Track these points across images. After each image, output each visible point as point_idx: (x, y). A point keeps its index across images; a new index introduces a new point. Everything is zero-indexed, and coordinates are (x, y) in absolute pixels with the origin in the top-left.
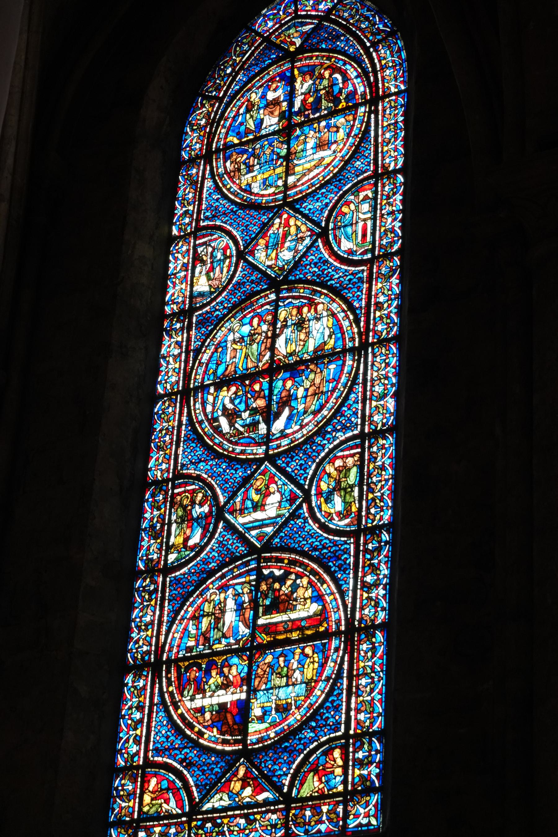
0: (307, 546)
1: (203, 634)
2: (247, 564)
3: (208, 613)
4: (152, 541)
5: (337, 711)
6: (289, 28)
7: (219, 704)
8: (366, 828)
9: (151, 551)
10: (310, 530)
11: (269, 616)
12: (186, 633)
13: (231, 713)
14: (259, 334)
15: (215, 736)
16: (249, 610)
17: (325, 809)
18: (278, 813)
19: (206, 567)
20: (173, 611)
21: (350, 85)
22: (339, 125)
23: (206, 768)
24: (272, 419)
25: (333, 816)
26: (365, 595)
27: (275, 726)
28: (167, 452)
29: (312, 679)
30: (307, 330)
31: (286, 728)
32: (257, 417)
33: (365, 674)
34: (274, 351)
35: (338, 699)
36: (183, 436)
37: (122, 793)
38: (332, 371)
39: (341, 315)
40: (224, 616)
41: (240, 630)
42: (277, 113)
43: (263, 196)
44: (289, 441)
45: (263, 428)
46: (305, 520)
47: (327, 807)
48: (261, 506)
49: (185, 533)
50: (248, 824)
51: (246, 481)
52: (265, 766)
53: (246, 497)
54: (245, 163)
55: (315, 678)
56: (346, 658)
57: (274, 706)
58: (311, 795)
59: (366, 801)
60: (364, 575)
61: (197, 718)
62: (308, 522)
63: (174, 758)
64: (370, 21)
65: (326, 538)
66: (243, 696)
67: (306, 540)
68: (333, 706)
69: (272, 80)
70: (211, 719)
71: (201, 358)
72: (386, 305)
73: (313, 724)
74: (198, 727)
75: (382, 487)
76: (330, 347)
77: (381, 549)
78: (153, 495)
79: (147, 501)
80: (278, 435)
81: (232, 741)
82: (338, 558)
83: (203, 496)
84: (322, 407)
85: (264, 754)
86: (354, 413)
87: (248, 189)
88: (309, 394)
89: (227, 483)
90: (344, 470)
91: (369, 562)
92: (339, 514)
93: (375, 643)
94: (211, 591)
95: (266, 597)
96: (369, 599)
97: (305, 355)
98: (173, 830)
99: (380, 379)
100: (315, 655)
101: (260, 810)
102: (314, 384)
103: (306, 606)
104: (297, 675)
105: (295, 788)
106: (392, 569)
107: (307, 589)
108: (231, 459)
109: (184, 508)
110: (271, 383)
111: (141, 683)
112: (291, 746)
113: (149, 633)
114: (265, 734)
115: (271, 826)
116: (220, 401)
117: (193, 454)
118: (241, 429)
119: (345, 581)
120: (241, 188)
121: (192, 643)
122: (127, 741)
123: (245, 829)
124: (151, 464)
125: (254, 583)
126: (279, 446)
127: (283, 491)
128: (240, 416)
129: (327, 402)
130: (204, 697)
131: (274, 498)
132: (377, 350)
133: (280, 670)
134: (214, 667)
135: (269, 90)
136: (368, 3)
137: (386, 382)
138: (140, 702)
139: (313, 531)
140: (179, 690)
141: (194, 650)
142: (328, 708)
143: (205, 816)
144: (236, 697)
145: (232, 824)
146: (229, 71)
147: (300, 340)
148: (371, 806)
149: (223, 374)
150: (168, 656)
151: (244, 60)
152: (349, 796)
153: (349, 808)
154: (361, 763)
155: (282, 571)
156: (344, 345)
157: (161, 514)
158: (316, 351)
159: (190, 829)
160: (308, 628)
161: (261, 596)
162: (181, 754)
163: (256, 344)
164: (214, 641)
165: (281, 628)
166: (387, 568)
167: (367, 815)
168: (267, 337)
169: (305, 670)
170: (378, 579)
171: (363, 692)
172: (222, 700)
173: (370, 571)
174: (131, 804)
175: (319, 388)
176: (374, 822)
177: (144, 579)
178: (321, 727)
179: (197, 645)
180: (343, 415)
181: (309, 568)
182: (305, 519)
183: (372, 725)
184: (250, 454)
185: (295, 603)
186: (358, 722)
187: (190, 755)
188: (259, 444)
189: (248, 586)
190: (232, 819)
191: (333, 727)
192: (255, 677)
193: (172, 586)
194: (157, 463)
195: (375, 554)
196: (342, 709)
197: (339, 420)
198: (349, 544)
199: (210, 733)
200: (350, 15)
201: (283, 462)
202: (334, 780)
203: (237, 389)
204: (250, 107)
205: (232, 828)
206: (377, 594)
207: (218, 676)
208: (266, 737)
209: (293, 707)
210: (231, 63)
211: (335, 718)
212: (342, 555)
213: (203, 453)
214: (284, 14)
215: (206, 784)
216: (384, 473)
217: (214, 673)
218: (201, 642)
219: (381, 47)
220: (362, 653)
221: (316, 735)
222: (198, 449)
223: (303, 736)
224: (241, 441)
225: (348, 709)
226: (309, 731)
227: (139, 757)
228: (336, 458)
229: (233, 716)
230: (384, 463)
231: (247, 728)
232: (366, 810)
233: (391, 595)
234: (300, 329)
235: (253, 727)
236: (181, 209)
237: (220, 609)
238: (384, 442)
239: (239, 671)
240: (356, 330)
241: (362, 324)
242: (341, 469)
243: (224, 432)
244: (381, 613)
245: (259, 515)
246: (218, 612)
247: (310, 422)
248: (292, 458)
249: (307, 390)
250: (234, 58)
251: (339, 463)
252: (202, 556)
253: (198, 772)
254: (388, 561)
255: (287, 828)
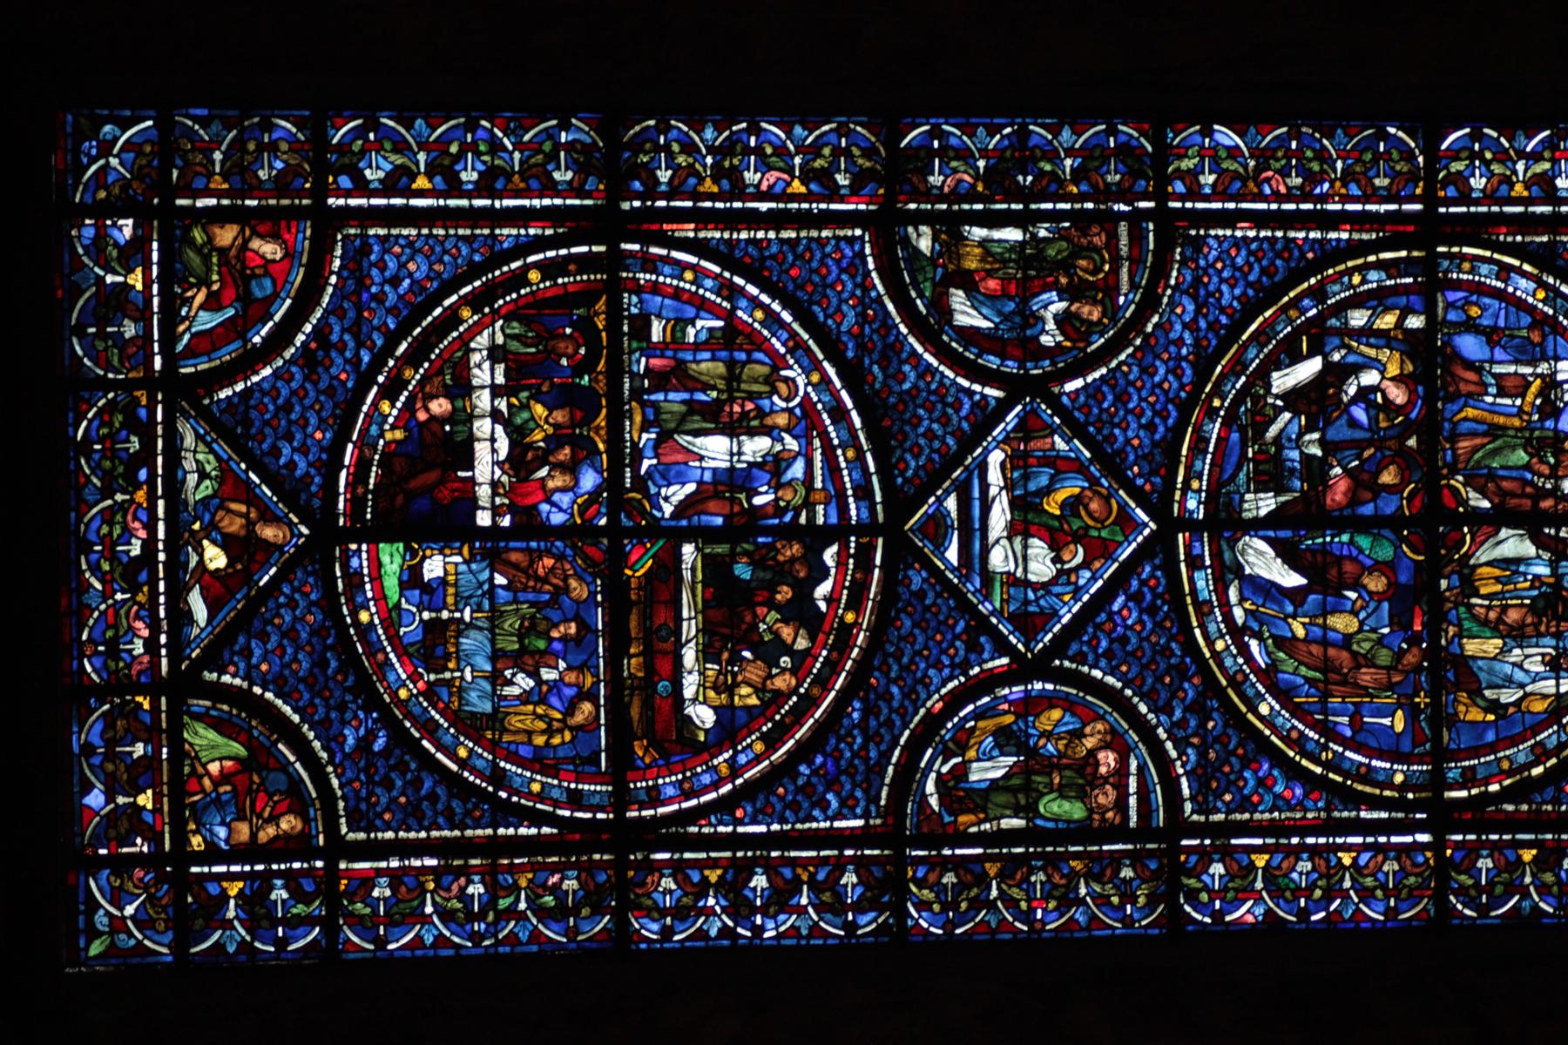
0: (883, 681)
1: (680, 368)
2: (863, 492)
3: (739, 379)
4: (981, 164)
5: (406, 816)
7: (471, 439)
8: (81, 924)
9: (954, 164)
10: (927, 686)
11: (700, 576)
12: (690, 312)
13: (442, 482)
14: (1554, 468)
15: (381, 435)
16: (726, 511)
17: (145, 800)
18: (146, 659)
19: (875, 356)
20: (763, 259)
23: (293, 416)
24: (1282, 534)
25: (124, 826)
26: (713, 875)
27: (391, 624)
28: (1251, 184)
29: (504, 730)
30: (1529, 630)
31: (380, 657)
32: (1297, 484)
33: (494, 890)
34: (1489, 525)
35: (436, 813)
36: (1292, 234)
37: (252, 146)
38: (1387, 721)
39: (1548, 736)
40: (721, 432)
41: (673, 489)
44: (1203, 595)
45: (1265, 504)
46: (959, 665)
47: (150, 806)
48: (1026, 522)
49: (989, 274)
50: (125, 566)
51: (1111, 462)
52: (281, 606)
53: (1061, 466)
55: (506, 738)
56: (546, 830)
57: (445, 615)
58: (187, 755)
59: (153, 921)
60: (771, 868)
61: (441, 372)
62: (951, 678)
63: (334, 310)
65: (895, 742)
66: (484, 519)
67: (899, 677)
68: (421, 800)
70: (432, 418)
71: (1524, 274)
72: (1549, 878)
73: (379, 744)
74: (414, 377)
75: (1012, 904)
76: (1462, 708)
77: (836, 914)
78: (1126, 151)
79: (1112, 131)
80: (1227, 556)
81: (360, 490)
82: (832, 784)
83: (1090, 323)
84: (1284, 695)
85: (313, 597)
86: (1248, 798)
88: (1332, 652)
89: (1117, 398)
90: (1082, 778)
91: (805, 877)
92: (961, 772)
93: (577, 915)
94: (801, 381)
95: (756, 563)
96: (703, 888)
97: (1452, 630)
98: (130, 330)
99: (1329, 877)
100: (568, 736)
101: (162, 599)
102: (1359, 667)
103: (711, 694)
104: (524, 682)
105: (208, 703)
106: (776, 951)
107: (759, 690)
108: (1185, 409)
109: (1066, 265)
110: (1394, 523)
111: (562, 176)
112: (327, 678)
113: (709, 186)
114: (370, 595)
115: (116, 638)
116: (1372, 352)
117: (1225, 274)
118: (1272, 431)
119: (762, 811)
121: (657, 331)
122: (401, 147)
123: (113, 557)
124: (1226, 136)
125: (803, 520)
126: (1195, 563)
127: (1057, 589)
128: (1310, 428)
129: (1297, 711)
130: (496, 391)
131: (1041, 567)
132: (1421, 859)
133: (542, 626)
134: (579, 415)
137: (1318, 893)
138: (508, 175)
139: (923, 696)
140: (527, 306)
141: (635, 345)
142: (417, 783)
143: (160, 430)
144: (484, 492)
145: (129, 518)
147: (1505, 609)
148: (140, 937)
149: (1458, 357)
150: (631, 253)
152: (172, 866)
153: (138, 873)
154: (255, 903)
155: (823, 606)
156: (1458, 755)
157: (1061, 183)
158: (1463, 663)
159: (128, 386)
160: (648, 704)
161: (759, 546)
162: (343, 331)
163: (1526, 458)
164: (654, 404)
165: (662, 616)
166: (779, 936)
167: (117, 925)
168: (1542, 493)
169: (531, 707)
170: (755, 910)
171: (449, 890)
172: (482, 450)
173: (780, 883)
174: (218, 183)
175: (1344, 683)
176: (96, 948)
177: (869, 152)
178: (366, 770)
179: (650, 350)
180: (1246, 763)
181: (816, 691)
182: (965, 666)
183: (357, 922)
184: (1188, 468)
185: (725, 655)
186: (368, 881)
187: (339, 361)
188: (1210, 502)
189: (798, 501)
190: (143, 516)
191: (363, 806)
192: (529, 550)
193: (837, 248)
194: (1223, 154)
195: (826, 897)
196: (408, 830)
197: (1233, 753)
198: (866, 815)
199: (391, 420)
201: (1143, 583)
202: (218, 819)
203: (1400, 409)
205: (119, 517)
206: (709, 912)
207: (551, 431)
208: (359, 599)
209: (432, 677)
211: (387, 809)
212: (838, 795)
213: (1223, 310)
215: (247, 423)
216: (1052, 904)
217: (560, 416)
218: (656, 362)
220: (555, 878)
221: (346, 756)
222: (1237, 292)
223: (348, 715)
224: (1235, 436)
225: (405, 849)
226: (362, 732)
227: (348, 194)
228: (1124, 753)
229: (430, 489)
230: (1082, 902)
231: (391, 540)
232: (129, 923)
233: (704, 954)
234: (1541, 604)
235: (392, 558)
237: (744, 415)
238: (1142, 900)
239: (556, 497)
240: (1494, 788)
241: (1510, 808)
242: (1089, 770)
243: (1275, 375)
244: (655, 927)
245: (999, 517)
246: (737, 409)
247: (1250, 659)
248: (1152, 610)
249: (1348, 638)
251: (1108, 759)
252: (911, 339)
253: (284, 392)
254: (800, 936)
255: (102, 693)
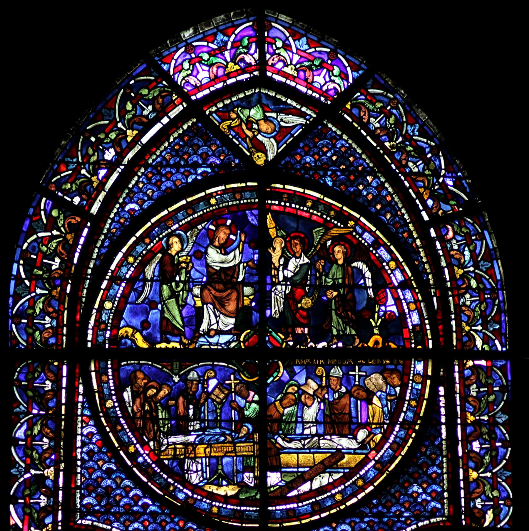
6: (248, 103)
21: (391, 301)
22: (372, 388)
42: (231, 306)
43: (212, 496)
54: (166, 407)
64: (427, 162)
69: (216, 217)
87: (177, 469)
120: (159, 463)
135: (212, 243)
136: (423, 116)
146: (110, 155)
151: (145, 140)
200: (383, 128)
204: (168, 268)
210: (113, 136)
214: (233, 59)
219: (451, 234)
236: (27, 471)
250: (120, 125)
